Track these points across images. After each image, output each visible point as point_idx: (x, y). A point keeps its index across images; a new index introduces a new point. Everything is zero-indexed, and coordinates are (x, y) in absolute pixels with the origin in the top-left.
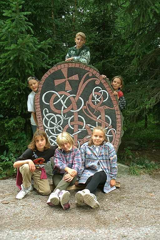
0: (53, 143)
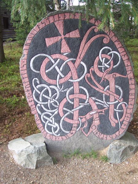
0: (48, 122)
